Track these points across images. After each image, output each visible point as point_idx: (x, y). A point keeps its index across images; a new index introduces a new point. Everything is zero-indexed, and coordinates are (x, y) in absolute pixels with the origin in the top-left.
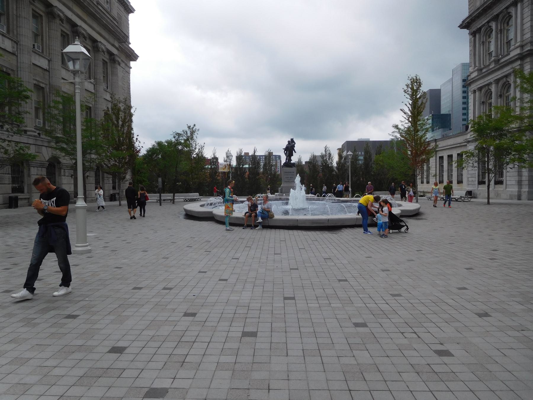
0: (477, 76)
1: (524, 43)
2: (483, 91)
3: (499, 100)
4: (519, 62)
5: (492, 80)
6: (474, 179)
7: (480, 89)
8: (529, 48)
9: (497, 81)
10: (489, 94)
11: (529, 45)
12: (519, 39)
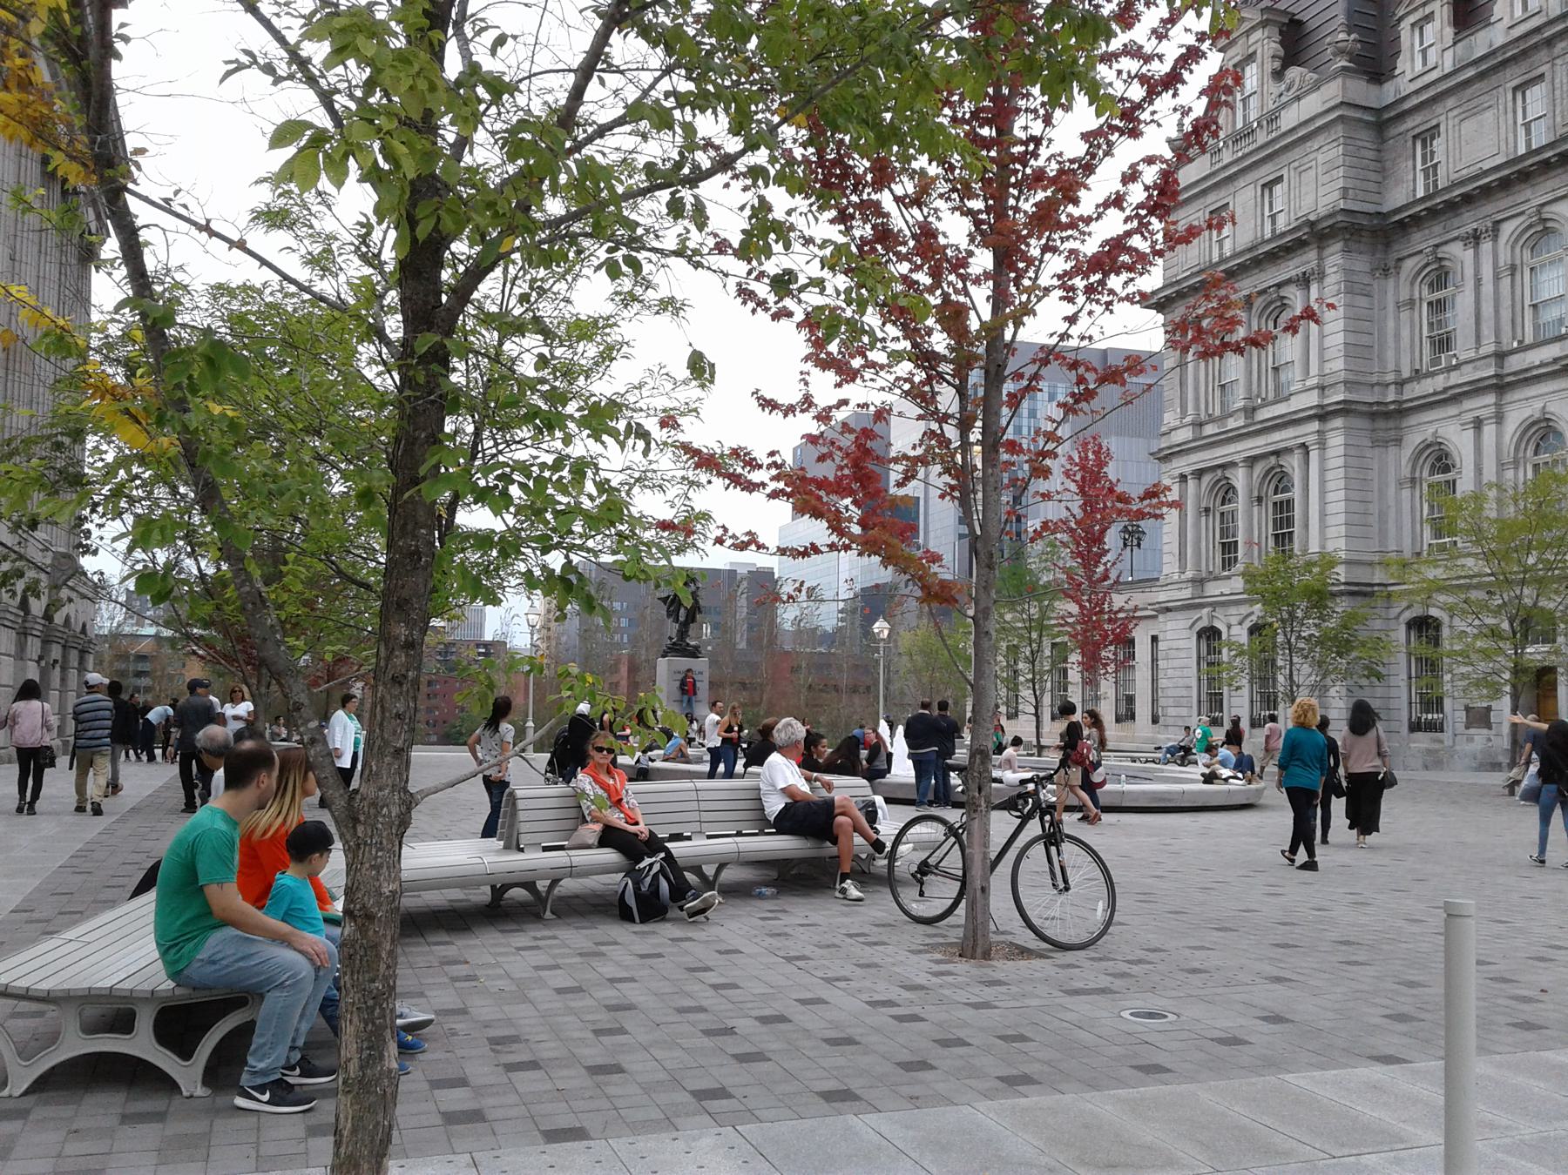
0: (1194, 440)
1: (1328, 381)
2: (1206, 479)
3: (1256, 509)
4: (1315, 426)
5: (1236, 458)
6: (1184, 712)
7: (1199, 474)
8: (1341, 397)
9: (1252, 461)
10: (1227, 492)
11: (1341, 387)
12: (1314, 370)
